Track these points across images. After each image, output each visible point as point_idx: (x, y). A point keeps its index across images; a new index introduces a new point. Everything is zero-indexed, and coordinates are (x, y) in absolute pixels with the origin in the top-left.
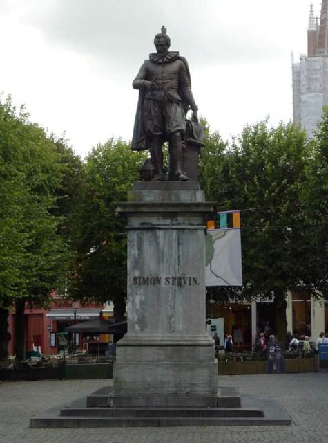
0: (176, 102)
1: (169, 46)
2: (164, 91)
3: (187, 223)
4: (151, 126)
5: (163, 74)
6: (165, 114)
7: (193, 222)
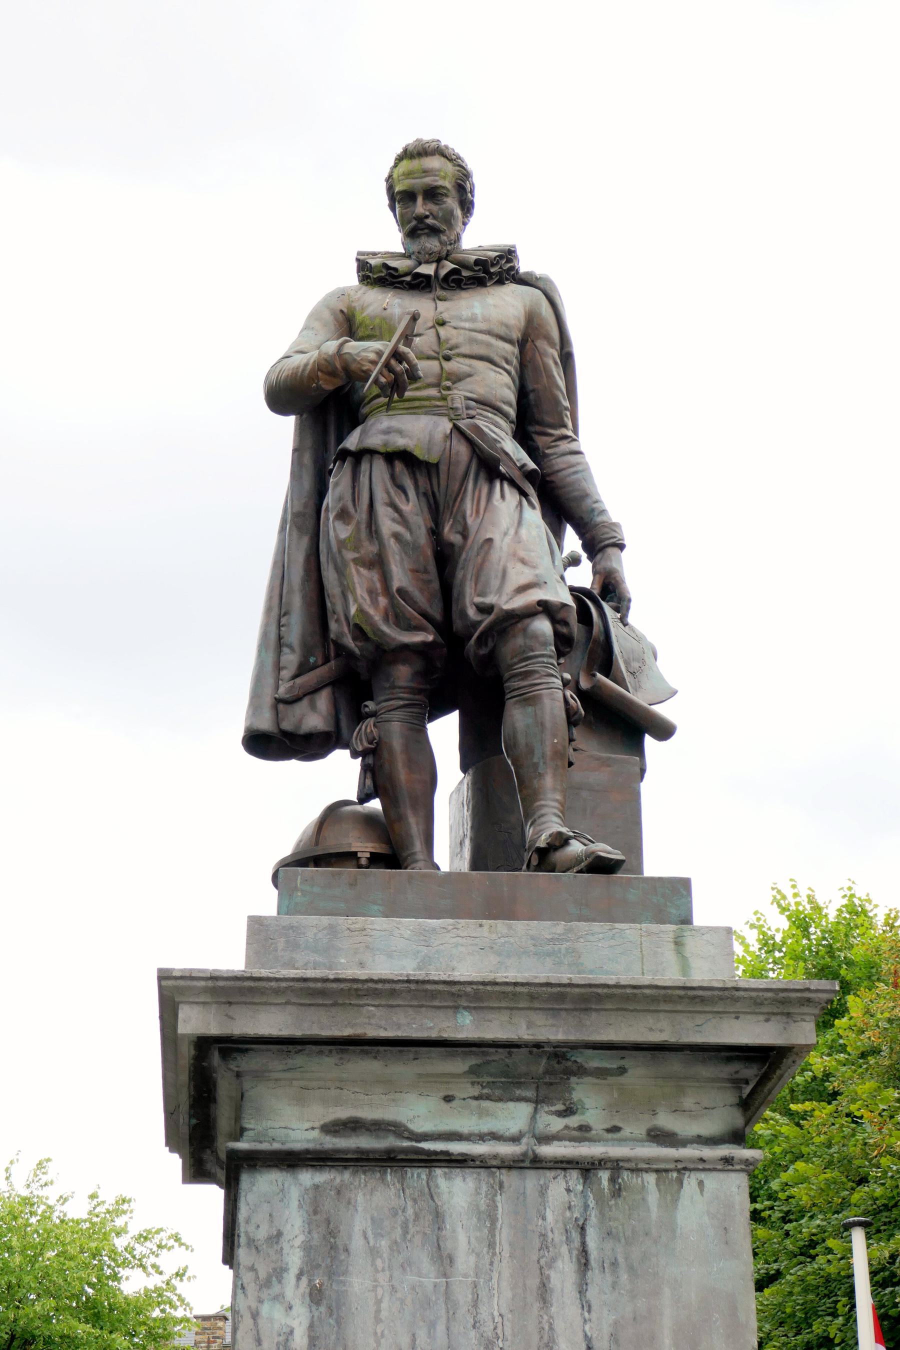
0: (513, 483)
1: (467, 207)
2: (452, 414)
3: (635, 1128)
4: (371, 592)
5: (442, 331)
6: (450, 534)
7: (666, 1121)
